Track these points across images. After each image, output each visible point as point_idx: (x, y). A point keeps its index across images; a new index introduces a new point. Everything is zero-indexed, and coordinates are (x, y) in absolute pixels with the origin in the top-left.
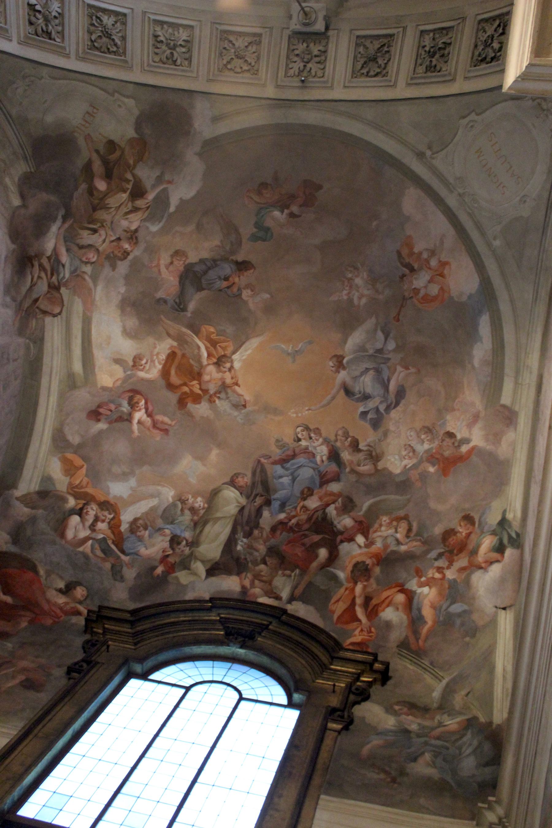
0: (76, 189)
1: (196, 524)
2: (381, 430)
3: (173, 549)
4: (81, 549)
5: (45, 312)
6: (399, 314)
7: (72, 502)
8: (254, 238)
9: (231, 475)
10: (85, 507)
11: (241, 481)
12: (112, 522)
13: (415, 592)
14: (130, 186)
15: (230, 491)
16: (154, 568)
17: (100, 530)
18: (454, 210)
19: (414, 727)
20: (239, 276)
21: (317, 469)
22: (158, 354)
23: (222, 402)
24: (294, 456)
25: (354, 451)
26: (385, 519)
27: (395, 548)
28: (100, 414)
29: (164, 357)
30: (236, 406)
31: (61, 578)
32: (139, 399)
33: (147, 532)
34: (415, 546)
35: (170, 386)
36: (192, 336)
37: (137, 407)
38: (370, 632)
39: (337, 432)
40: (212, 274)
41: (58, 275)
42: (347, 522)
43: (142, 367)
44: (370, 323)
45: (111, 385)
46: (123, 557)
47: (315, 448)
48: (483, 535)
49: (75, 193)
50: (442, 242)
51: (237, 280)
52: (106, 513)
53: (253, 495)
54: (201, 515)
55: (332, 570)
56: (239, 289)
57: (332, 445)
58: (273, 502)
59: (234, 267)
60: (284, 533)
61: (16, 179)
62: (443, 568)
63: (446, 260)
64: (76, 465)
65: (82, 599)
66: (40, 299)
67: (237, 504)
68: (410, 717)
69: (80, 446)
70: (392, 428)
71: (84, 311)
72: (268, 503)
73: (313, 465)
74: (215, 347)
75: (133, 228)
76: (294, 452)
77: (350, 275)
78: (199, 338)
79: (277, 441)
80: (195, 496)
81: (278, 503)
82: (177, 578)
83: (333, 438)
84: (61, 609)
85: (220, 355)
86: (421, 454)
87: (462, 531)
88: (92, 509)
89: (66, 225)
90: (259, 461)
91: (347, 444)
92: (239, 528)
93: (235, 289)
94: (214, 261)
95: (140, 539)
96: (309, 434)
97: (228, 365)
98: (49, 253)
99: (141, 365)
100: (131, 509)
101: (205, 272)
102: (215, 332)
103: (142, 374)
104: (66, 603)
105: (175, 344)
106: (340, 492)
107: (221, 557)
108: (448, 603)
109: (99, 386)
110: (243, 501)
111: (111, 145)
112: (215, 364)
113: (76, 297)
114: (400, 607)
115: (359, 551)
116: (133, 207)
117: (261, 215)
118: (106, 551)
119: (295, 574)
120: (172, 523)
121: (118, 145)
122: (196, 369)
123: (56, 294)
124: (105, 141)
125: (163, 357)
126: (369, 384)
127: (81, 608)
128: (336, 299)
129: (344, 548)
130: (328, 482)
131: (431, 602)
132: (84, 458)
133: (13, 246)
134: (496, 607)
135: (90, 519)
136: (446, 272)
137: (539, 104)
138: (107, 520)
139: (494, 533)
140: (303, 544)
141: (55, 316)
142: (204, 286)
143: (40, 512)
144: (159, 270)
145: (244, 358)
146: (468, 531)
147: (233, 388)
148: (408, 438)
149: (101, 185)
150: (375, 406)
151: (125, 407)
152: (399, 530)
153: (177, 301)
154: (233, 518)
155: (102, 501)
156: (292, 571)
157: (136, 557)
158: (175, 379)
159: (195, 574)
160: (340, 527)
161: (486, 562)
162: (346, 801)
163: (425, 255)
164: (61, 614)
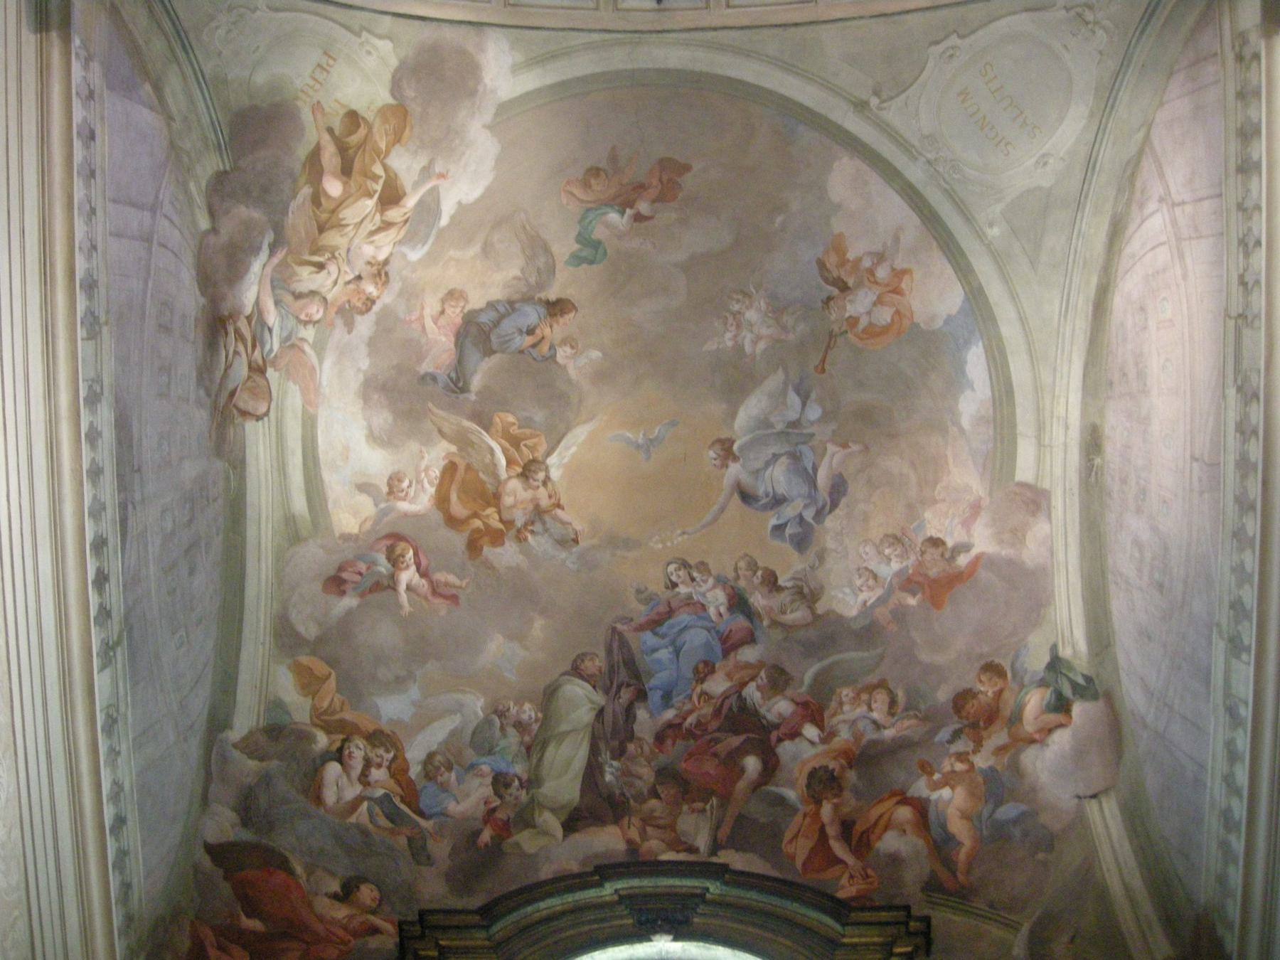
1: (528, 749)
2: (811, 553)
3: (501, 797)
4: (353, 819)
5: (245, 414)
6: (823, 361)
7: (322, 741)
8: (577, 260)
9: (573, 657)
10: (346, 746)
11: (590, 666)
12: (394, 766)
13: (928, 800)
14: (379, 187)
15: (578, 685)
16: (477, 834)
17: (376, 782)
18: (920, 187)
20: (551, 327)
21: (714, 628)
22: (426, 470)
23: (539, 538)
24: (670, 613)
25: (770, 591)
26: (846, 693)
28: (344, 582)
29: (438, 473)
31: (332, 874)
32: (403, 550)
33: (453, 775)
34: (908, 728)
35: (452, 522)
36: (480, 433)
37: (402, 563)
38: (868, 876)
39: (736, 564)
40: (508, 326)
43: (403, 495)
44: (774, 381)
45: (355, 530)
46: (423, 822)
47: (704, 595)
49: (292, 204)
50: (896, 239)
51: (547, 331)
52: (381, 751)
53: (615, 686)
54: (535, 732)
55: (773, 788)
56: (552, 347)
57: (732, 588)
58: (650, 694)
59: (542, 311)
60: (678, 742)
61: (204, 184)
62: (968, 753)
63: (905, 266)
64: (319, 675)
65: (374, 905)
66: (239, 389)
67: (590, 705)
69: (320, 640)
70: (830, 544)
71: (303, 406)
72: (642, 695)
73: (706, 624)
74: (517, 447)
75: (382, 257)
76: (670, 607)
77: (736, 307)
78: (491, 436)
79: (639, 591)
80: (519, 702)
81: (660, 693)
82: (517, 845)
83: (731, 575)
84: (345, 928)
85: (526, 460)
86: (889, 579)
87: (987, 689)
88: (358, 747)
89: (275, 260)
90: (614, 630)
91: (756, 581)
92: (602, 745)
93: (545, 348)
94: (511, 303)
95: (444, 788)
96: (689, 574)
97: (541, 475)
98: (248, 310)
99: (403, 491)
100: (420, 737)
101: (497, 323)
102: (517, 423)
103: (404, 506)
104: (351, 917)
105: (453, 448)
106: (759, 661)
107: (582, 797)
108: (990, 806)
109: (337, 535)
110: (600, 699)
111: (353, 118)
113: (291, 384)
114: (908, 828)
116: (383, 221)
117: (587, 221)
118: (394, 816)
119: (712, 806)
120: (490, 752)
121: (363, 118)
122: (490, 488)
123: (261, 381)
124: (342, 112)
125: (436, 472)
127: (377, 921)
128: (715, 347)
130: (736, 647)
131: (960, 811)
132: (329, 663)
133: (202, 301)
135: (357, 765)
136: (903, 285)
137: (1079, 15)
138: (386, 763)
139: (1042, 683)
140: (715, 755)
141: (259, 418)
142: (495, 347)
143: (274, 764)
145: (566, 460)
146: (996, 689)
148: (861, 557)
149: (333, 187)
150: (796, 513)
151: (383, 567)
152: (874, 706)
153: (453, 375)
154: (590, 729)
155: (371, 731)
156: (706, 801)
157: (443, 819)
159: (545, 833)
160: (772, 717)
161: (1040, 731)
163: (867, 263)
164: (349, 937)
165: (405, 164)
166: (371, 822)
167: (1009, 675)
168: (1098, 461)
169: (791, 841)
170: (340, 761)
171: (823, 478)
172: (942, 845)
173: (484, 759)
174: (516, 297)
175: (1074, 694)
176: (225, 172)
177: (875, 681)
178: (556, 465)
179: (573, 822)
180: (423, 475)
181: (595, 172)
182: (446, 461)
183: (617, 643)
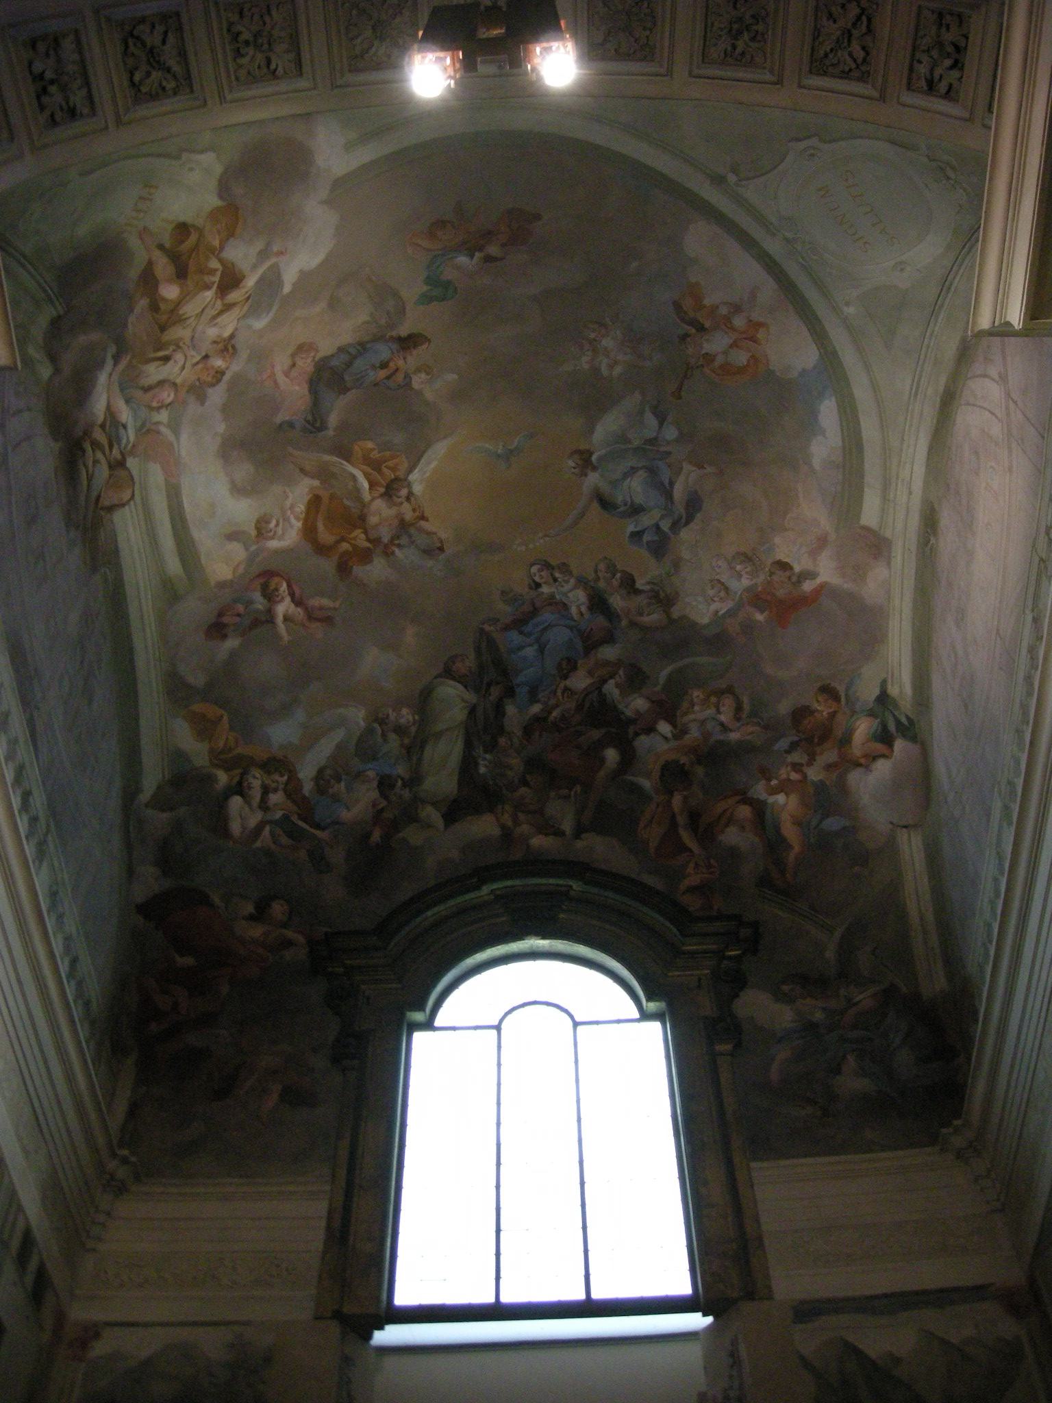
0: (131, 310)
1: (409, 750)
4: (258, 844)
6: (680, 389)
7: (222, 778)
8: (427, 299)
11: (461, 667)
13: (764, 803)
14: (216, 278)
16: (367, 836)
17: (275, 805)
19: (819, 1016)
22: (292, 507)
24: (535, 611)
26: (697, 694)
28: (225, 626)
30: (428, 552)
32: (277, 584)
33: (343, 784)
34: (752, 733)
35: (322, 550)
37: (278, 596)
40: (359, 364)
41: (119, 444)
42: (638, 704)
43: (272, 534)
44: (632, 401)
45: (229, 577)
46: (318, 833)
48: (855, 717)
51: (401, 363)
52: (276, 777)
54: (413, 735)
55: (631, 778)
58: (518, 690)
59: (395, 346)
62: (802, 765)
63: (762, 320)
66: (102, 493)
67: (463, 704)
68: (808, 1001)
70: (686, 554)
71: (166, 479)
72: (510, 692)
74: (379, 471)
75: (227, 334)
77: (592, 336)
78: (353, 465)
79: (503, 592)
81: (526, 689)
87: (823, 708)
88: (255, 777)
90: (482, 631)
91: (615, 583)
93: (400, 377)
94: (362, 344)
95: (336, 799)
96: (552, 575)
97: (404, 492)
99: (271, 531)
101: (349, 364)
102: (376, 447)
103: (274, 544)
105: (316, 483)
106: (619, 660)
109: (213, 583)
110: (471, 697)
111: (183, 229)
112: (382, 496)
115: (664, 746)
116: (224, 305)
118: (294, 833)
119: (576, 792)
120: (374, 758)
121: (193, 226)
123: (123, 473)
124: (170, 227)
125: (301, 508)
126: (639, 489)
127: (289, 934)
129: (643, 742)
133: (57, 446)
134: (891, 823)
135: (256, 794)
136: (759, 336)
139: (871, 714)
144: (275, 382)
145: (428, 474)
147: (418, 525)
150: (653, 522)
151: (260, 603)
152: (722, 709)
153: (310, 418)
156: (571, 790)
157: (337, 826)
158: (325, 536)
159: (429, 826)
160: (629, 713)
161: (866, 756)
162: (783, 1162)
163: (724, 310)
165: (240, 253)
166: (274, 843)
167: (843, 699)
168: (933, 541)
169: (646, 827)
170: (241, 794)
171: (678, 492)
172: (775, 845)
173: (370, 766)
174: (366, 339)
175: (897, 732)
176: (59, 317)
177: (724, 686)
178: (418, 481)
179: (454, 812)
180: (289, 512)
181: (441, 224)
182: (311, 495)
183: (486, 645)
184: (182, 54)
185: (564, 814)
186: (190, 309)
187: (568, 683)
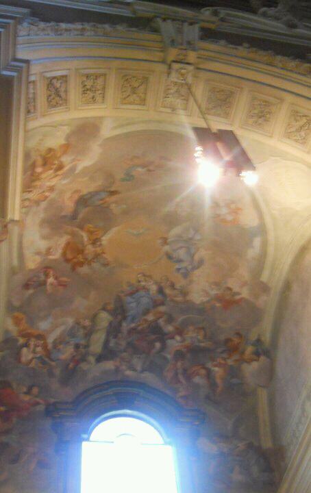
7: (21, 341)
16: (69, 364)
24: (137, 291)
26: (191, 328)
27: (197, 344)
35: (67, 261)
42: (170, 328)
46: (53, 364)
70: (195, 279)
103: (51, 257)
105: (69, 237)
111: (50, 150)
118: (43, 362)
120: (73, 337)
125: (63, 245)
127: (38, 400)
129: (169, 342)
135: (32, 347)
151: (43, 277)
165: (66, 160)
172: (213, 385)
178: (105, 240)
183: (119, 300)
184: (66, 91)
185: (138, 362)
186: (44, 176)
187: (145, 317)
